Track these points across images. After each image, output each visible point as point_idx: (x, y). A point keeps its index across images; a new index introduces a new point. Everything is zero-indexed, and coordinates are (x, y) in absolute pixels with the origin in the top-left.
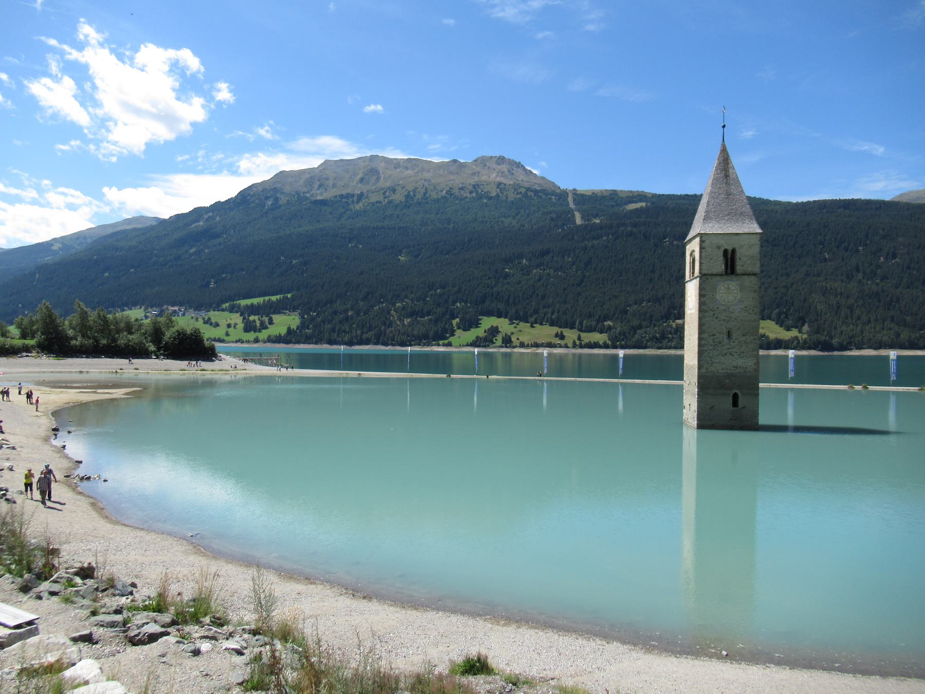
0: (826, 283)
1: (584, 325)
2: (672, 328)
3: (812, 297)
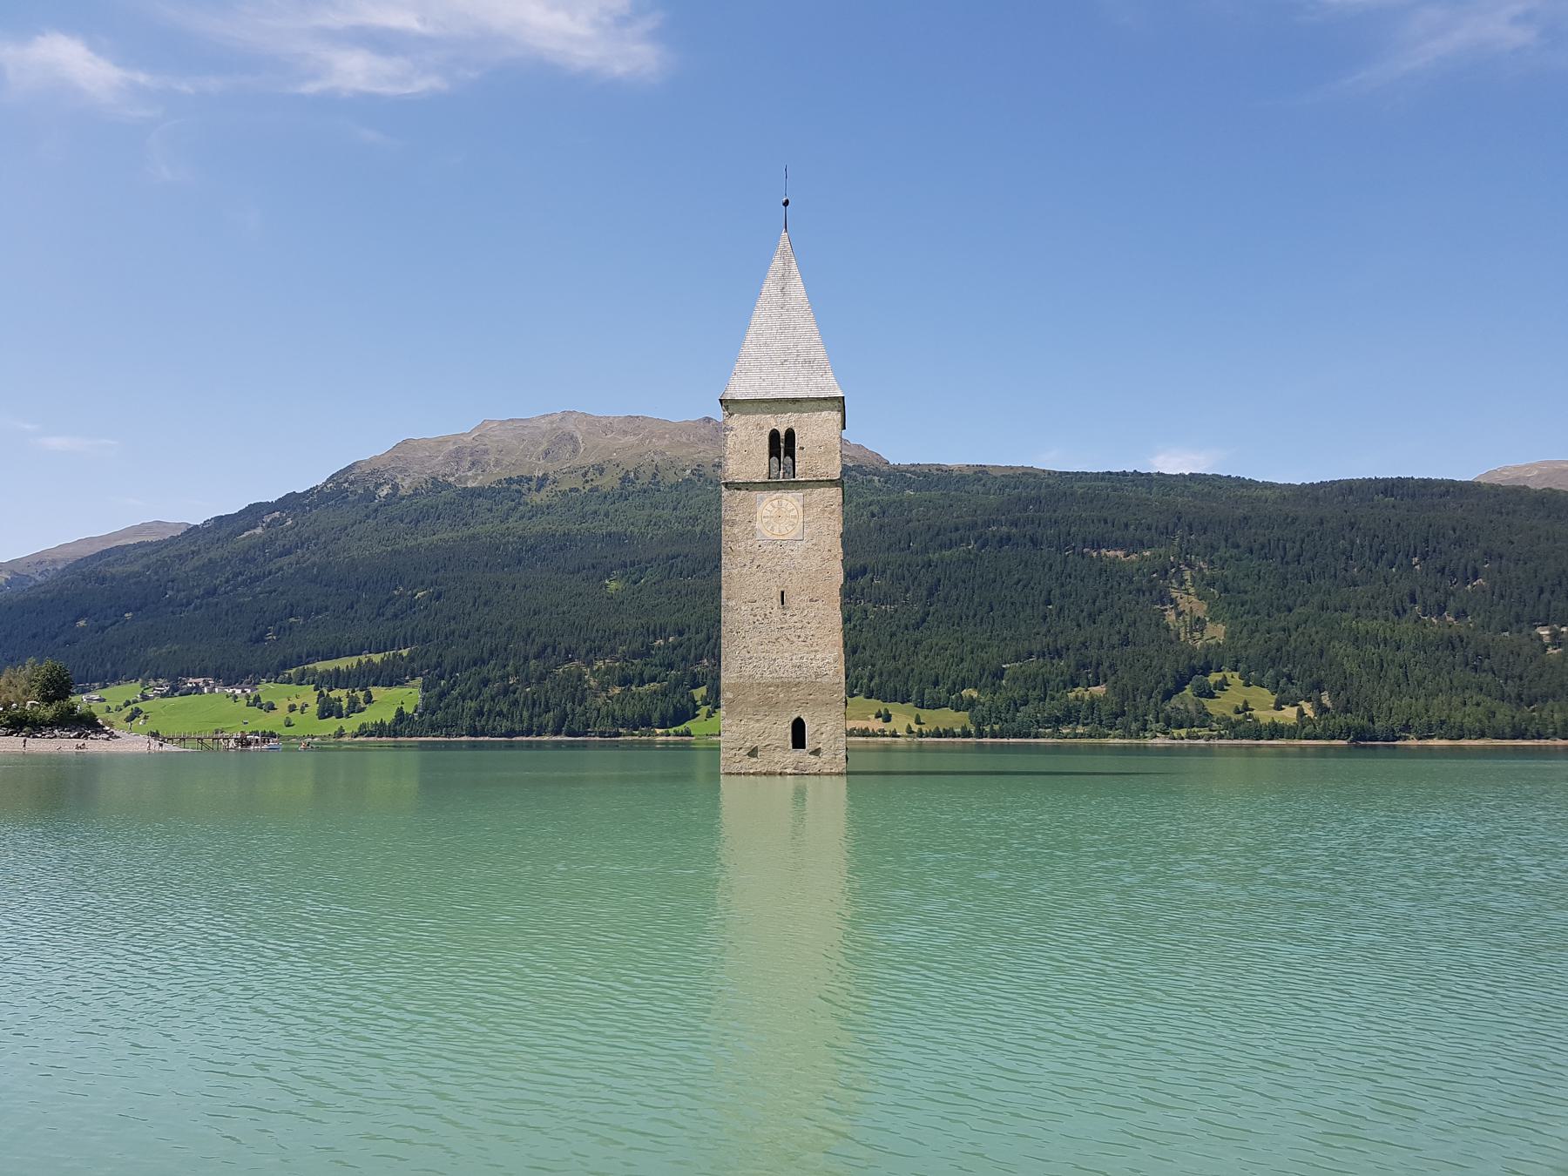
0: (1357, 622)
1: (926, 697)
2: (1083, 701)
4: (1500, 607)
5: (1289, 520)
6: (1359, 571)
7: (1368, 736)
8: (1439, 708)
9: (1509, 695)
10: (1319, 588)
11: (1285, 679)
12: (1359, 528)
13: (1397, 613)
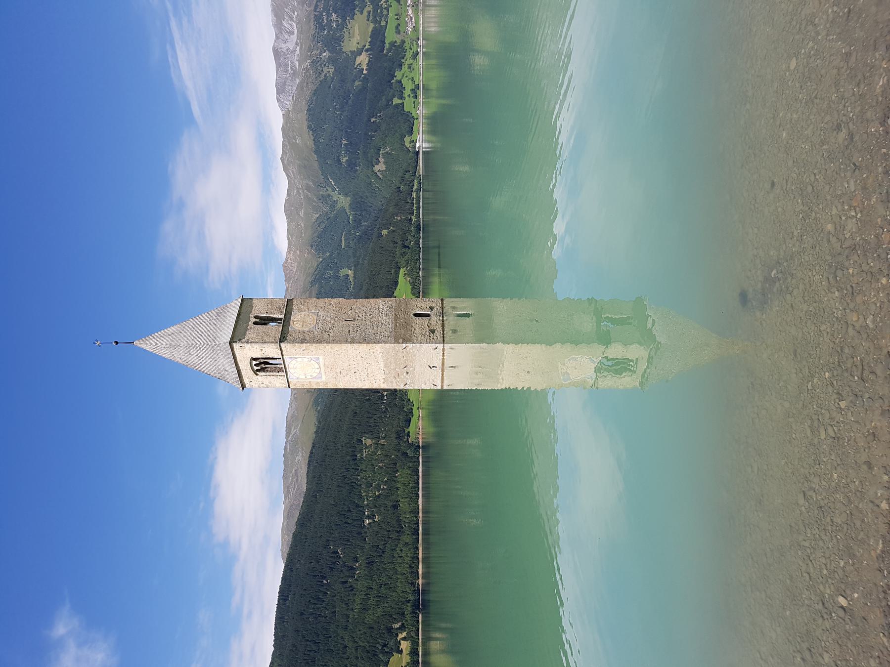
3: (368, 621)
4: (353, 541)
5: (294, 649)
6: (328, 610)
7: (417, 603)
8: (403, 568)
9: (398, 536)
10: (335, 631)
11: (385, 648)
12: (304, 610)
13: (353, 590)
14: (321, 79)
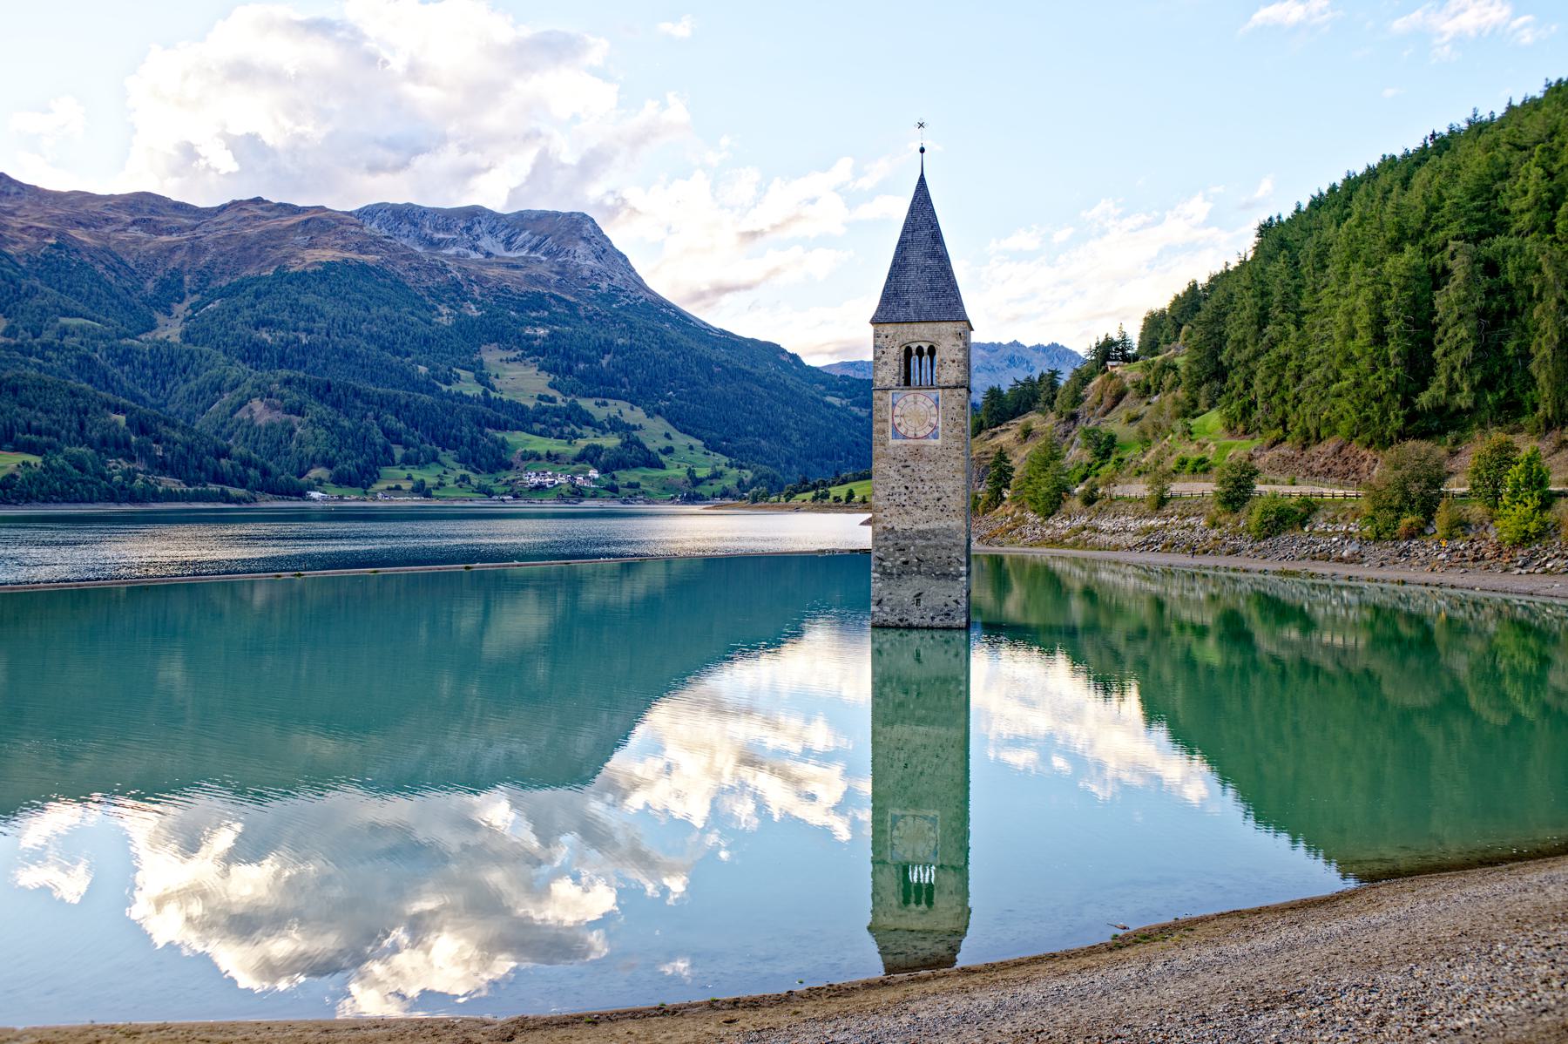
14: (427, 299)
